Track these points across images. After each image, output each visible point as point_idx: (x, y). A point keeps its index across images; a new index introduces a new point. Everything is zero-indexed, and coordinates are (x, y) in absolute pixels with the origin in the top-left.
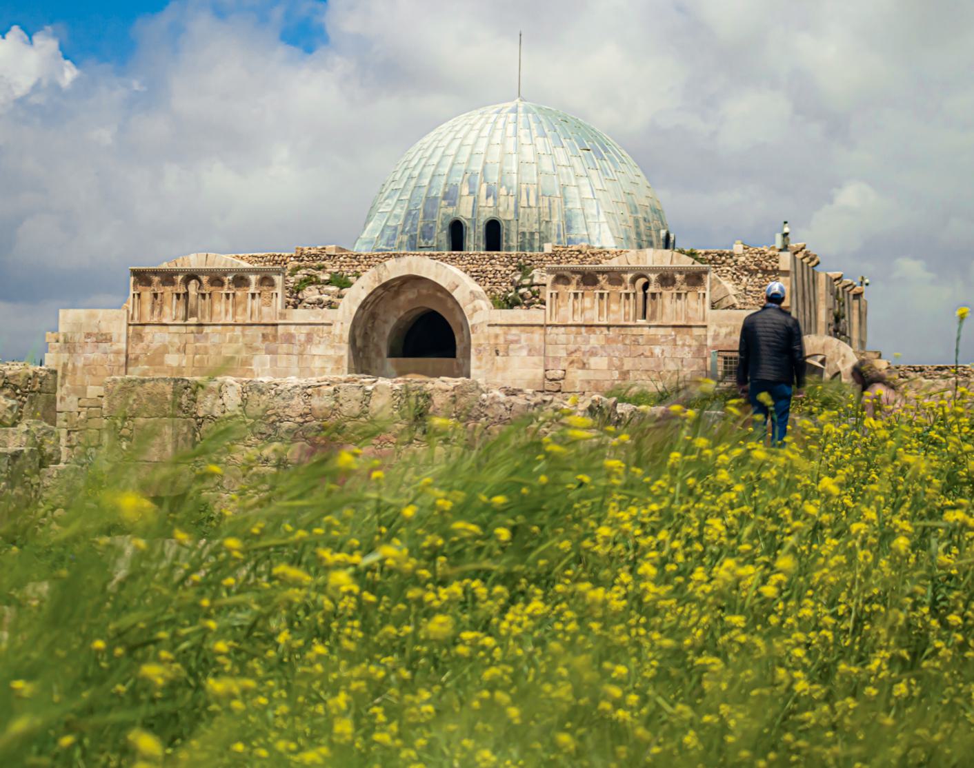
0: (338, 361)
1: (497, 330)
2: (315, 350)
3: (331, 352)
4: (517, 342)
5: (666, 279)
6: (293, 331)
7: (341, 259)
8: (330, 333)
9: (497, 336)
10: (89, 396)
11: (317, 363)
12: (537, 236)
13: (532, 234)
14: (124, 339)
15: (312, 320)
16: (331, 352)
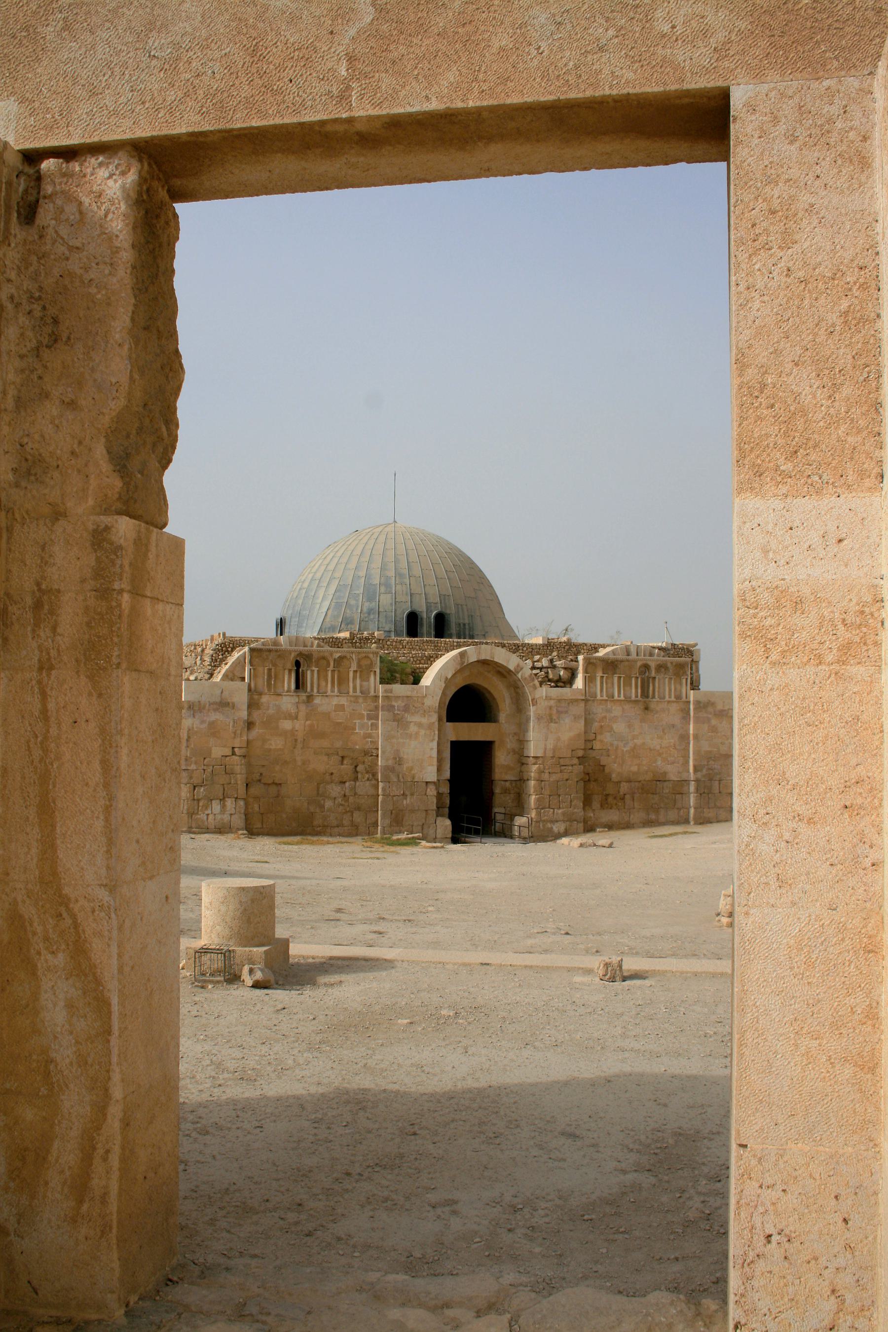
0: (430, 726)
1: (552, 703)
2: (409, 718)
3: (424, 721)
4: (566, 712)
5: (661, 667)
6: (394, 703)
7: (389, 643)
8: (423, 704)
9: (550, 708)
10: (213, 756)
11: (413, 729)
12: (467, 627)
13: (464, 625)
14: (245, 707)
15: (409, 694)
16: (424, 721)
